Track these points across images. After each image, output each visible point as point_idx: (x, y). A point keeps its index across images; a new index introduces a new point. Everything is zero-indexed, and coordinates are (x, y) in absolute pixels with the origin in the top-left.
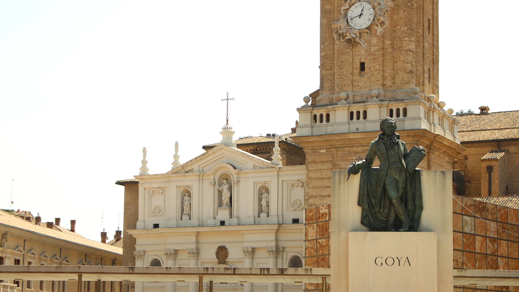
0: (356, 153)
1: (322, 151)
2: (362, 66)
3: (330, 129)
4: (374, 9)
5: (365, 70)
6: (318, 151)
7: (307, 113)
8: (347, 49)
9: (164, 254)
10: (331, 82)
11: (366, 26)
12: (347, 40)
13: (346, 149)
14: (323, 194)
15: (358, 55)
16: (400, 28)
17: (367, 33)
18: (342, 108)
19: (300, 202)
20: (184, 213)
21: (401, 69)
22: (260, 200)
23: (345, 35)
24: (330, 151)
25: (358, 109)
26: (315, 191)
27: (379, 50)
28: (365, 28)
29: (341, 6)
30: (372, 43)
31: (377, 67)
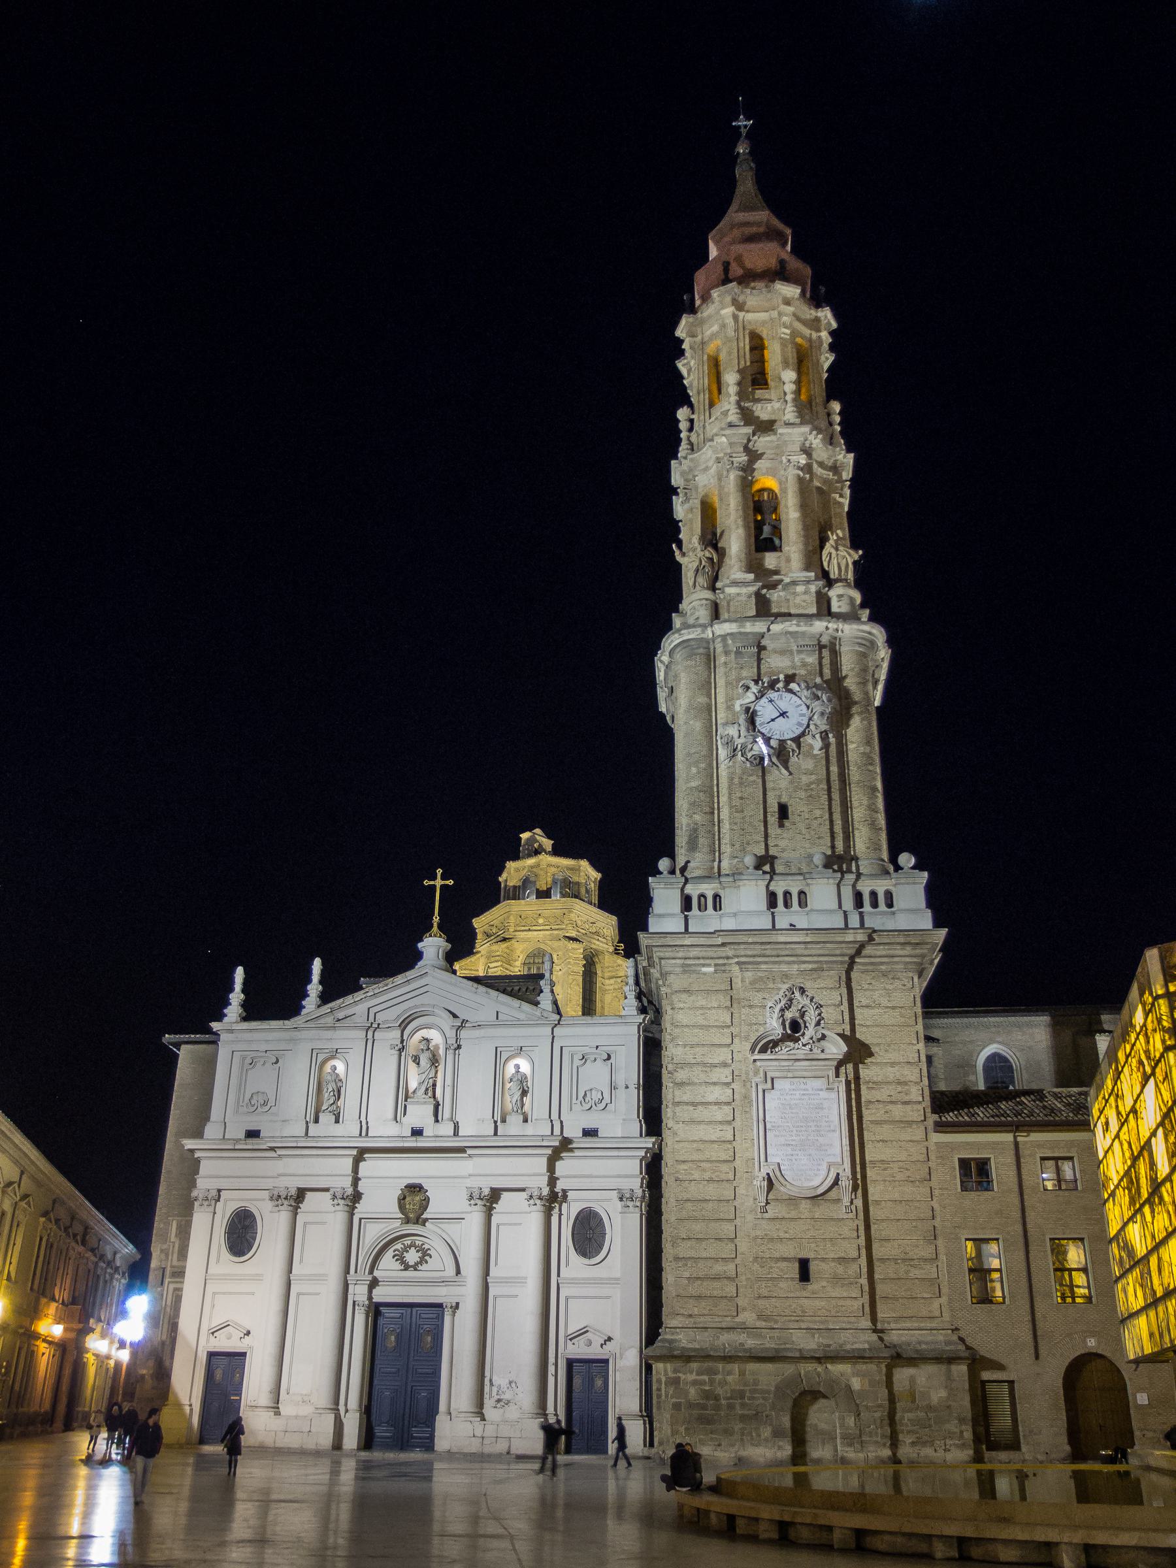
0: (786, 976)
1: (704, 969)
2: (783, 811)
3: (729, 924)
6: (698, 968)
7: (673, 888)
8: (751, 775)
9: (268, 1198)
11: (792, 736)
13: (763, 966)
18: (754, 883)
19: (600, 1093)
20: (324, 1108)
24: (724, 971)
25: (789, 886)
27: (818, 782)
28: (791, 739)
31: (818, 813)
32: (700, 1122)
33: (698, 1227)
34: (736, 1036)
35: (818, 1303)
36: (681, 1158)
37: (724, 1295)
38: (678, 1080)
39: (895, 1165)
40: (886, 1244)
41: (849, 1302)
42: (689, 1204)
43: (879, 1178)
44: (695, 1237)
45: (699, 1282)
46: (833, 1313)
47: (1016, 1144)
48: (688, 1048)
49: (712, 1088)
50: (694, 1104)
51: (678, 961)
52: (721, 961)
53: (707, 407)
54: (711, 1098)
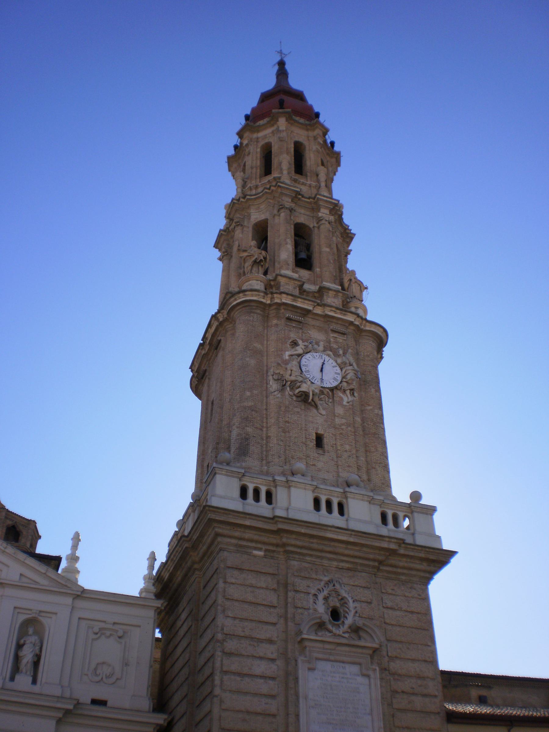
1: (256, 552)
2: (319, 441)
4: (341, 369)
5: (326, 446)
6: (249, 551)
7: (233, 477)
8: (296, 407)
10: (261, 449)
12: (300, 393)
13: (308, 558)
14: (258, 636)
15: (312, 422)
16: (372, 409)
17: (329, 398)
21: (380, 463)
22: (19, 646)
23: (298, 384)
24: (272, 557)
27: (348, 425)
28: (328, 388)
29: (282, 351)
30: (336, 411)
32: (246, 693)
48: (237, 621)
50: (240, 674)
51: (233, 541)
52: (271, 548)
53: (258, 176)
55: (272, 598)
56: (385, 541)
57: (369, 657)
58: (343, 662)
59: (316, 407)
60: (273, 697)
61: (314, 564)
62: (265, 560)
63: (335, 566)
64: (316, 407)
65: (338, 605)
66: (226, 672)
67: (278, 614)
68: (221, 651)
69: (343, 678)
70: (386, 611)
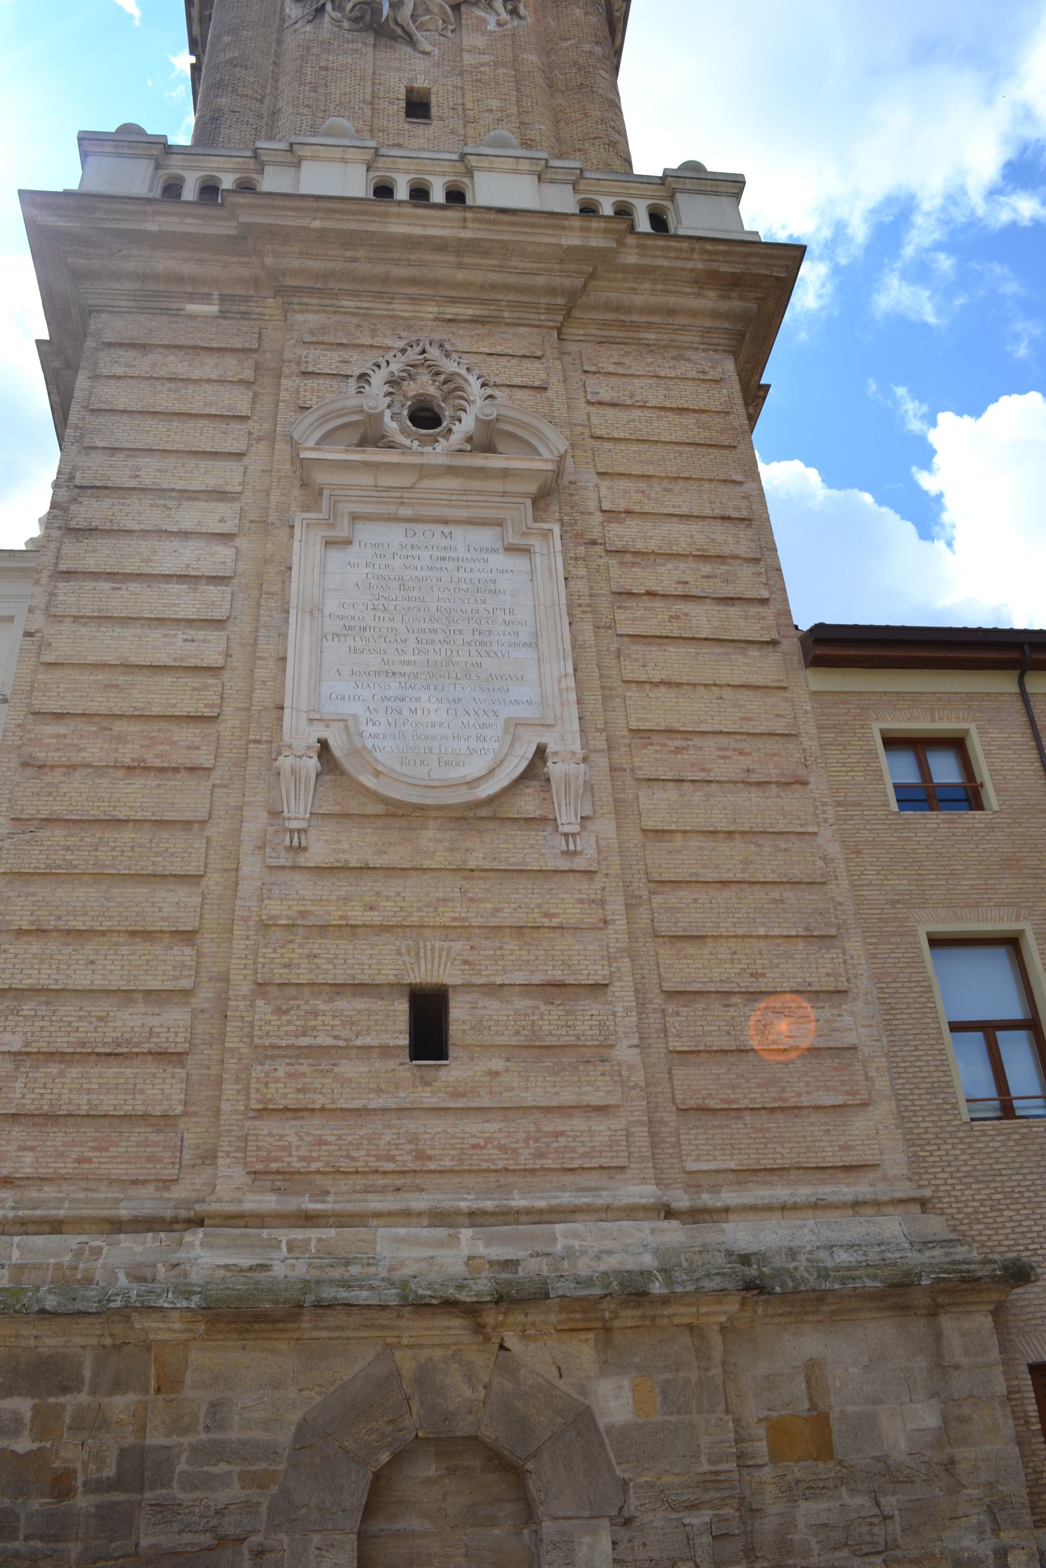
1: (192, 308)
7: (137, 157)
13: (348, 303)
18: (338, 153)
21: (595, 138)
24: (245, 315)
26: (125, 466)
33: (76, 895)
34: (259, 439)
35: (473, 1127)
36: (53, 706)
37: (140, 1109)
38: (73, 524)
39: (710, 743)
40: (690, 949)
41: (578, 1123)
42: (57, 835)
43: (662, 772)
44: (61, 924)
45: (54, 1069)
46: (525, 1158)
47: (1024, 697)
49: (176, 543)
54: (169, 566)
55: (239, 401)
56: (572, 228)
57: (529, 502)
58: (446, 522)
59: (411, 41)
60: (218, 623)
61: (366, 315)
62: (226, 322)
63: (431, 316)
64: (411, 41)
65: (432, 390)
66: (69, 575)
67: (250, 433)
68: (60, 528)
69: (443, 559)
70: (593, 410)
